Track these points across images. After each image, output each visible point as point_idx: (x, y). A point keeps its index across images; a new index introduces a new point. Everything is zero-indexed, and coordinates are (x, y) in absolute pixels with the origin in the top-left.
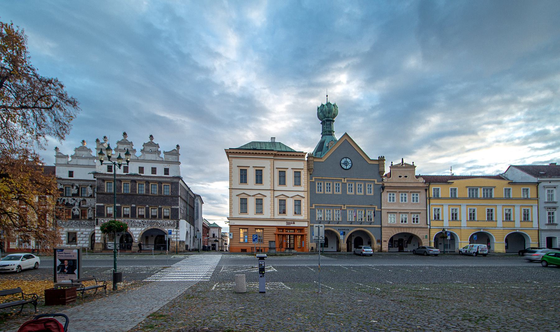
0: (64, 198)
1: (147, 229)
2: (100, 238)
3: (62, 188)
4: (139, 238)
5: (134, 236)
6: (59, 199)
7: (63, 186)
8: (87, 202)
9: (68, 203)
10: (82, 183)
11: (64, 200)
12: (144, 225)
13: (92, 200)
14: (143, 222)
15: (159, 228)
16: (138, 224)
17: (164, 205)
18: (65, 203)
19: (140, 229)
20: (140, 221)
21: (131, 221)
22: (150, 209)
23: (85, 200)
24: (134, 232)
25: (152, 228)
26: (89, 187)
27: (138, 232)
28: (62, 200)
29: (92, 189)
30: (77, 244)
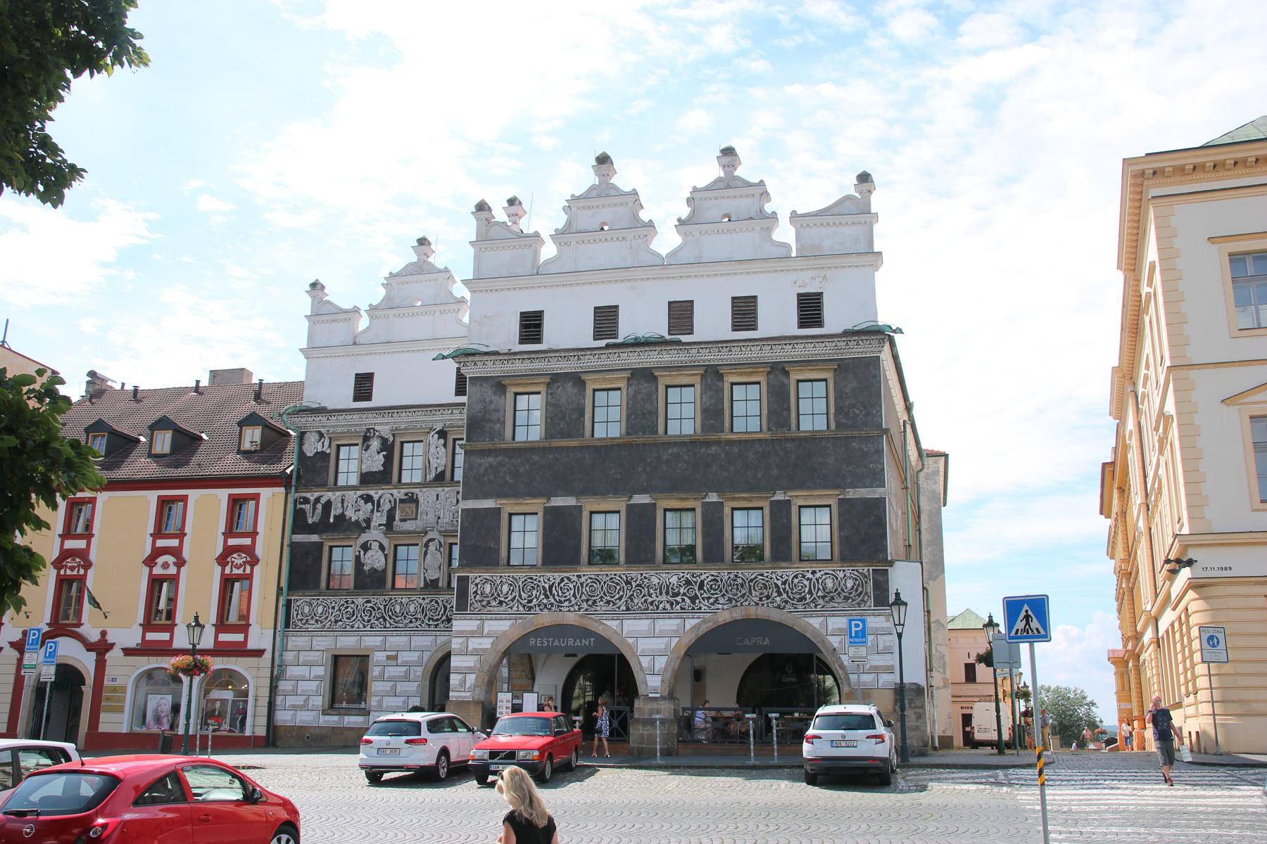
0: (328, 496)
1: (710, 625)
2: (471, 679)
3: (323, 453)
4: (668, 676)
5: (645, 662)
6: (306, 501)
7: (327, 444)
8: (422, 507)
9: (341, 518)
10: (403, 420)
11: (328, 505)
12: (693, 599)
13: (442, 495)
14: (688, 582)
15: (775, 615)
16: (664, 598)
17: (801, 487)
18: (332, 520)
19: (670, 624)
20: (674, 580)
21: (628, 583)
22: (727, 510)
23: (412, 500)
24: (644, 645)
25: (738, 614)
26: (434, 439)
27: (659, 644)
28: (319, 506)
29: (445, 445)
30: (366, 713)
